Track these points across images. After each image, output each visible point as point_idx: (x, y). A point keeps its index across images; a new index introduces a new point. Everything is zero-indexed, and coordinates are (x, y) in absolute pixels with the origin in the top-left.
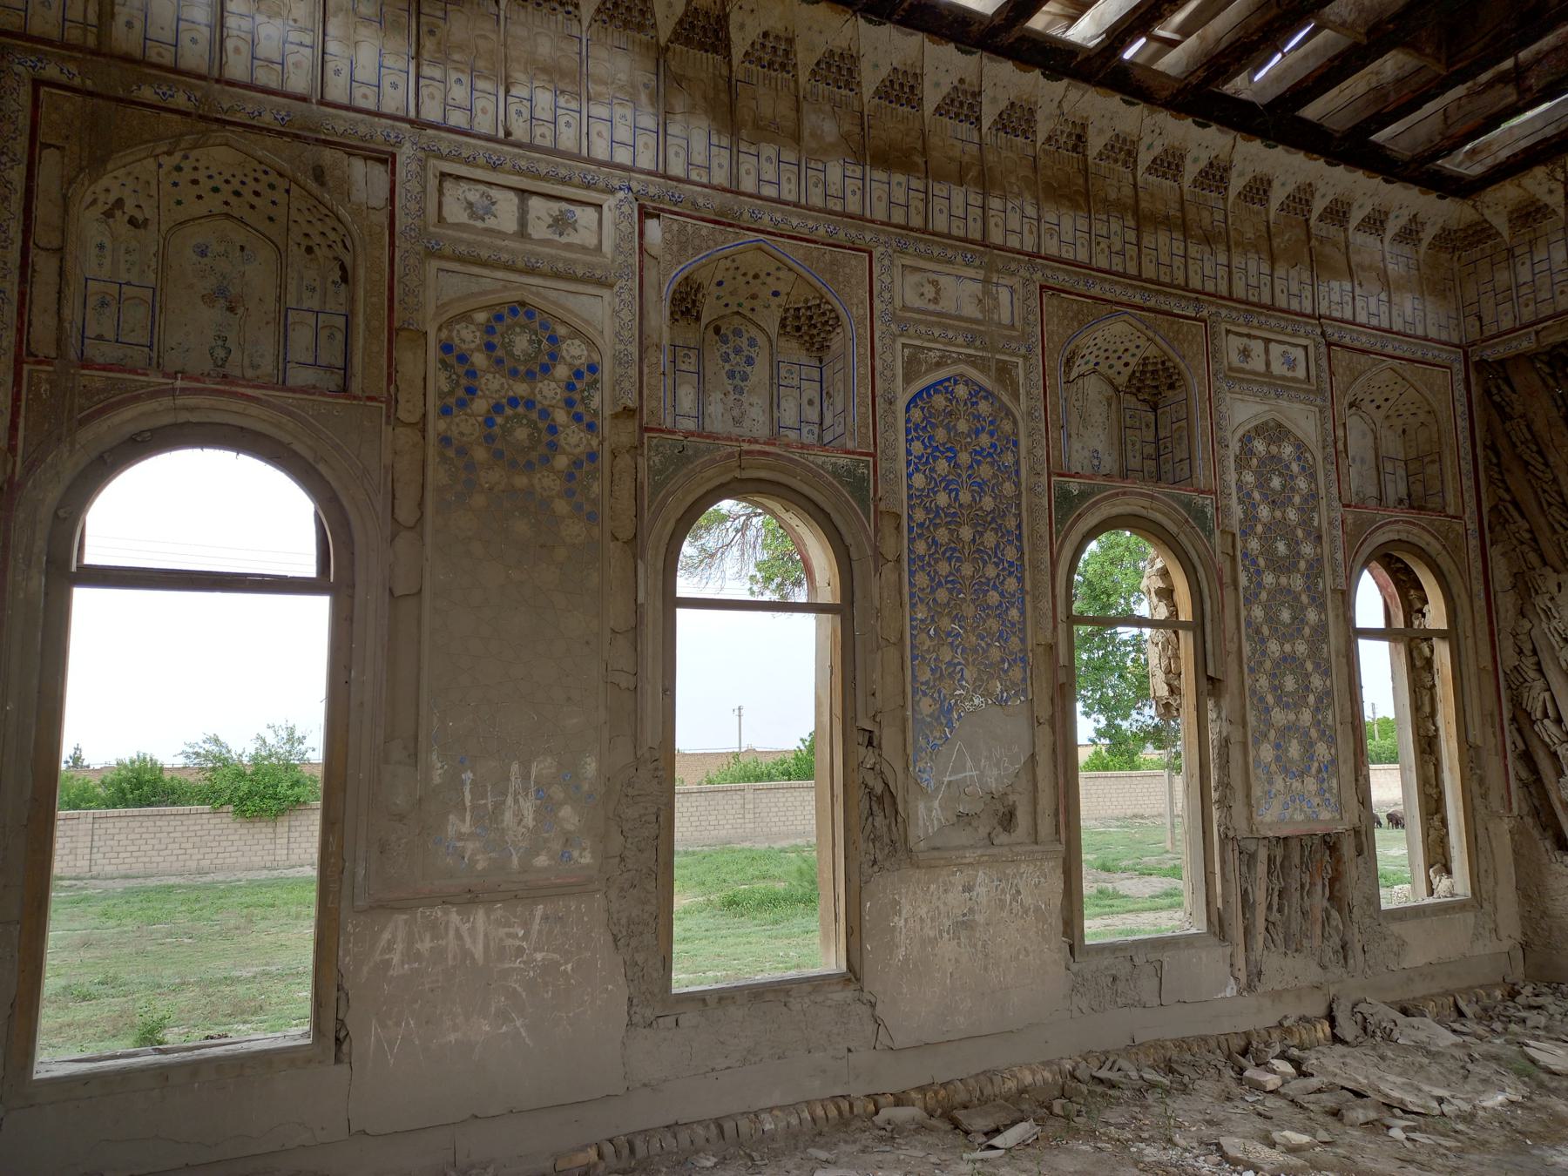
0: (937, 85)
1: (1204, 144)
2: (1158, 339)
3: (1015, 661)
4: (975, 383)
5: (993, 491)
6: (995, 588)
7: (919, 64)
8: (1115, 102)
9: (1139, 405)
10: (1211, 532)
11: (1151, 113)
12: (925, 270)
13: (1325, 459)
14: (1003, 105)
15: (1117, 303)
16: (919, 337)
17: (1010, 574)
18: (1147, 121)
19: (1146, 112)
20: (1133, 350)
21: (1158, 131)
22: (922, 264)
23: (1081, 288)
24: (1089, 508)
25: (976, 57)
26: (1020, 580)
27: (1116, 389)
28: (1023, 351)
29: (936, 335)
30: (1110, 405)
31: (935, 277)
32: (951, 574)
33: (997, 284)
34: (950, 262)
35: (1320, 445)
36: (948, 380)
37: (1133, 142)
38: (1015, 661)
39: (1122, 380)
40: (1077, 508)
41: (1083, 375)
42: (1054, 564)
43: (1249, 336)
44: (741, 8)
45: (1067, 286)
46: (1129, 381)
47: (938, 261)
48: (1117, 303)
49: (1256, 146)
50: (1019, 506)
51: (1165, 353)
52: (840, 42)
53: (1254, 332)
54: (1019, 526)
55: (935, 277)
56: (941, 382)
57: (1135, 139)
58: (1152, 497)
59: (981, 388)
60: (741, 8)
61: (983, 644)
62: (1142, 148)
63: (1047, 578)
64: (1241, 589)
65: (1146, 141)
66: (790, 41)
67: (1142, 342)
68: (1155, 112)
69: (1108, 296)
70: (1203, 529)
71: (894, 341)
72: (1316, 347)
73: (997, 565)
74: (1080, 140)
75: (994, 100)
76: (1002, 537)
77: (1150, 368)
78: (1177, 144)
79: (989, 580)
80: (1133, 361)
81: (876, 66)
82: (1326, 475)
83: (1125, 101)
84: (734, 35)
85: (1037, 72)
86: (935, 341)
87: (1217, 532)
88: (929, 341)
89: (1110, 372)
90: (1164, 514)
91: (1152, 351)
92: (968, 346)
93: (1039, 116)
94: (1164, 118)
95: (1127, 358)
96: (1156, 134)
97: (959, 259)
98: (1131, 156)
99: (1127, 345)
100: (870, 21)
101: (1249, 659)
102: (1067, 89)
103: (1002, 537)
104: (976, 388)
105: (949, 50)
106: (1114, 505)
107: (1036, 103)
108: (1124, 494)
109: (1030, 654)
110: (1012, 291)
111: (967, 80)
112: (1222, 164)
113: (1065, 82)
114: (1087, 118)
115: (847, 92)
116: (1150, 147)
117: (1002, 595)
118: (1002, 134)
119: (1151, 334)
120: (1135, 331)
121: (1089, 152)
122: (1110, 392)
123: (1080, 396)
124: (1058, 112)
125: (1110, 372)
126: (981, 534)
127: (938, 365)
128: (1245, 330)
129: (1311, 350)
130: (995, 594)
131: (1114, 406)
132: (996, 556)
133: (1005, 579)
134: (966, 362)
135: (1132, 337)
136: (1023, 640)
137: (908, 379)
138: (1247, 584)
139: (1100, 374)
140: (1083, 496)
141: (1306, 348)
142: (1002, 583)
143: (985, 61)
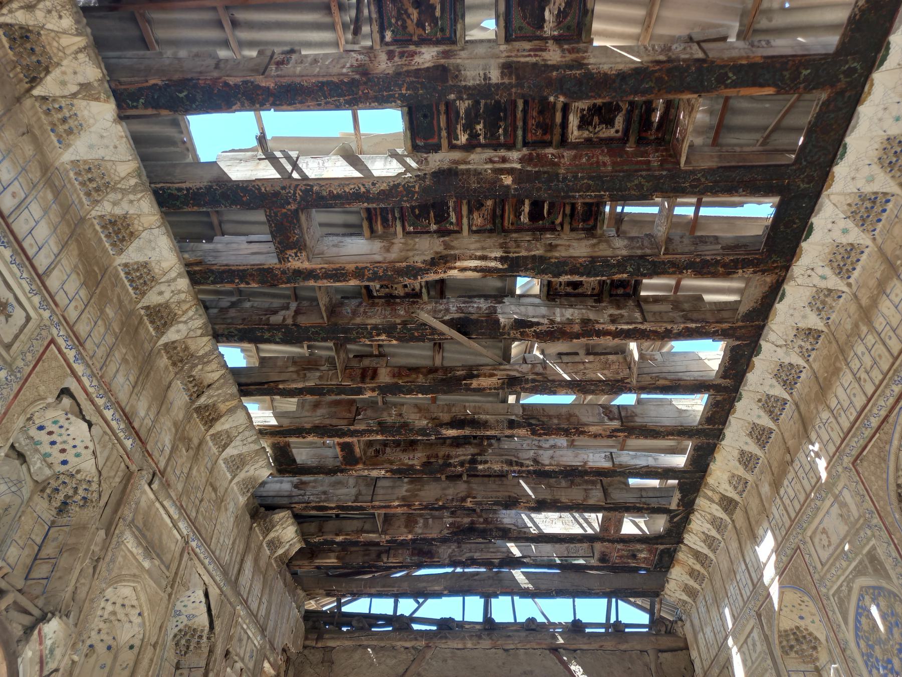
1: (830, 226)
8: (780, 308)
11: (793, 278)
16: (834, 582)
18: (799, 281)
19: (792, 283)
21: (809, 272)
23: (868, 433)
25: (743, 393)
45: (862, 443)
47: (816, 515)
49: (840, 170)
57: (815, 289)
62: (823, 284)
65: (816, 280)
69: (883, 413)
74: (811, 333)
75: (772, 386)
78: (827, 251)
81: (746, 443)
83: (781, 300)
93: (787, 361)
94: (798, 268)
96: (813, 274)
100: (723, 439)
105: (739, 405)
113: (762, 342)
124: (784, 348)
143: (746, 388)
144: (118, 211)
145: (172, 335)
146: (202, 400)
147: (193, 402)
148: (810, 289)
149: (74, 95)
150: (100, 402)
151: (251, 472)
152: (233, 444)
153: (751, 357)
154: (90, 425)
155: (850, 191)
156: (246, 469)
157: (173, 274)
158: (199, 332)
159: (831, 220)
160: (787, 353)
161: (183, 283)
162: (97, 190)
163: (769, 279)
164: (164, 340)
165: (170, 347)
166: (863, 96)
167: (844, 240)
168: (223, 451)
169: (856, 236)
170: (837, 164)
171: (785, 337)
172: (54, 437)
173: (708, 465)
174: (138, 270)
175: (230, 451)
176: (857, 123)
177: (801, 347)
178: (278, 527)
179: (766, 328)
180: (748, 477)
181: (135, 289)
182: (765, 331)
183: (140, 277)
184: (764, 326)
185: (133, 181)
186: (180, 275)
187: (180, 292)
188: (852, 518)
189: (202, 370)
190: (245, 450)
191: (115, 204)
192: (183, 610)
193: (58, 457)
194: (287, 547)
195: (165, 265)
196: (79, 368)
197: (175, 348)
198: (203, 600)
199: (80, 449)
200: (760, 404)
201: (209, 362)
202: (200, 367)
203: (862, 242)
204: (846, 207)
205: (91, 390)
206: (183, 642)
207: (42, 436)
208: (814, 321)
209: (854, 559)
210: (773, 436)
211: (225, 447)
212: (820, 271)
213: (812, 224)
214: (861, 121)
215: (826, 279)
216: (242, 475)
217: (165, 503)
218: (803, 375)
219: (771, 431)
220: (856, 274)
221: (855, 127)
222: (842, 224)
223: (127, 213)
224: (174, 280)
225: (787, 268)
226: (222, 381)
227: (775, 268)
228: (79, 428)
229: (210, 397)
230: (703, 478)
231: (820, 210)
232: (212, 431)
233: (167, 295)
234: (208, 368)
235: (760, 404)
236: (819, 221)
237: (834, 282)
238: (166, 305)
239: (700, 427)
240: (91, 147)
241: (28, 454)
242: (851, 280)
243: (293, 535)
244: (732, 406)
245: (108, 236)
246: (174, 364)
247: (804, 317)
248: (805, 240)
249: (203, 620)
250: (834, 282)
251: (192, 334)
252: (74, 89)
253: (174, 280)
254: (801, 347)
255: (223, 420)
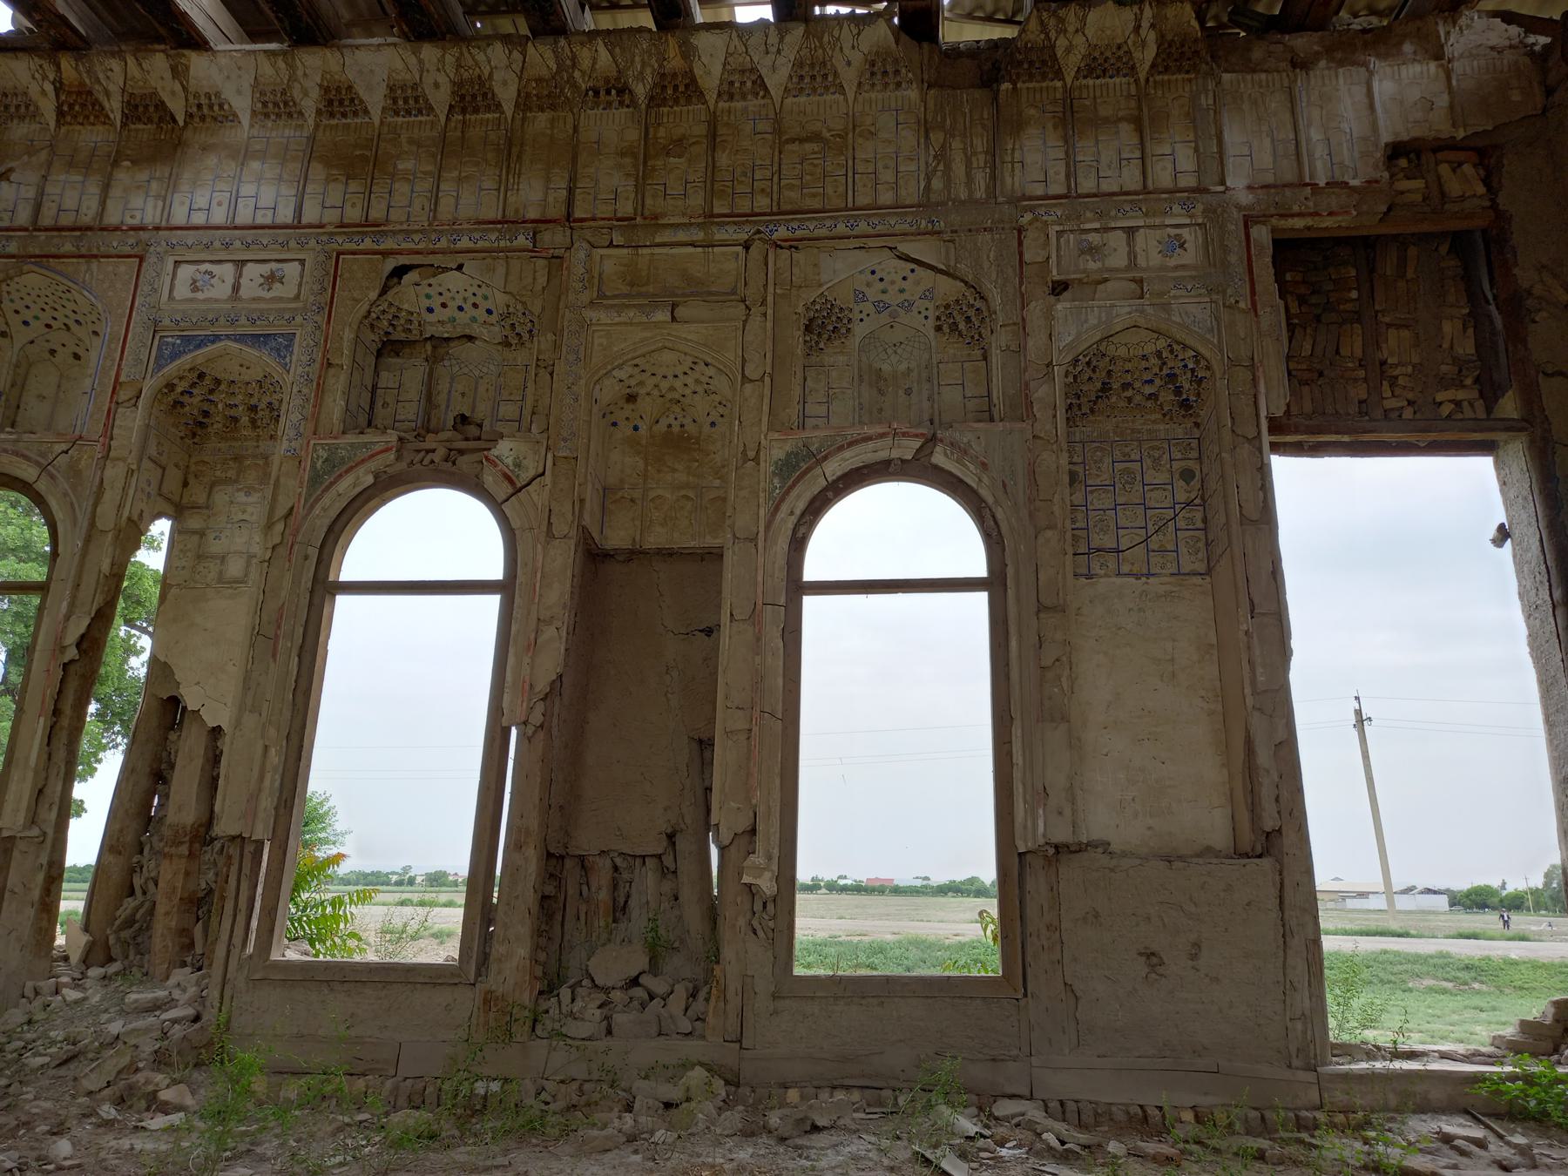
144: (315, 93)
145: (507, 94)
146: (641, 91)
147: (633, 103)
149: (185, 89)
150: (443, 243)
151: (857, 58)
152: (764, 72)
154: (460, 268)
156: (839, 63)
157: (413, 60)
158: (516, 55)
161: (429, 52)
162: (286, 104)
164: (508, 108)
165: (524, 103)
168: (766, 89)
172: (453, 305)
174: (395, 101)
175: (776, 81)
178: (1061, 43)
181: (420, 112)
183: (406, 101)
185: (281, 64)
186: (416, 53)
187: (442, 60)
189: (583, 73)
190: (790, 54)
191: (306, 94)
192: (905, 296)
193: (480, 314)
194: (1152, 37)
195: (399, 65)
196: (389, 244)
197: (528, 95)
198: (913, 266)
199: (479, 292)
201: (574, 58)
202: (577, 74)
205: (421, 246)
206: (962, 326)
207: (440, 314)
211: (760, 84)
216: (849, 77)
217: (658, 240)
223: (320, 86)
224: (421, 62)
226: (617, 50)
228: (452, 280)
229: (641, 77)
232: (711, 97)
233: (442, 79)
234: (586, 63)
238: (458, 85)
240: (239, 92)
241: (467, 332)
243: (1128, 14)
245: (344, 115)
246: (553, 107)
249: (948, 288)
251: (517, 67)
252: (178, 87)
253: (421, 62)
255: (698, 72)
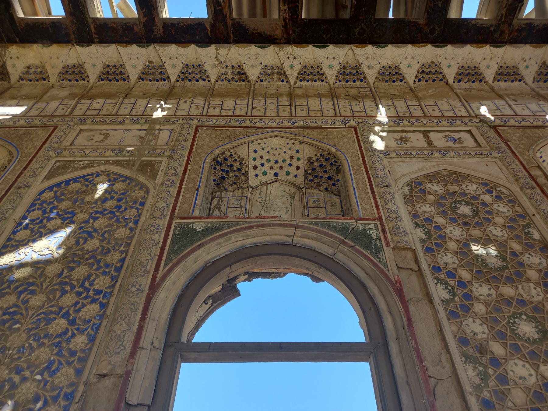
0: (134, 66)
2: (306, 139)
3: (55, 399)
4: (115, 174)
5: (103, 235)
6: (66, 316)
7: (120, 60)
8: (253, 49)
9: (322, 194)
10: (378, 251)
11: (281, 49)
12: (100, 130)
13: (521, 188)
14: (180, 67)
15: (266, 128)
17: (93, 301)
18: (281, 53)
19: (277, 50)
20: (296, 155)
21: (292, 57)
22: (97, 127)
24: (213, 240)
26: (103, 306)
27: (299, 188)
28: (167, 153)
29: (87, 152)
30: (292, 197)
31: (107, 132)
32: (15, 305)
33: (160, 130)
34: (120, 123)
35: (512, 179)
36: (92, 175)
37: (279, 68)
38: (55, 399)
39: (300, 180)
40: (198, 240)
41: (266, 184)
42: (154, 287)
43: (404, 131)
44: (11, 58)
45: (222, 124)
46: (306, 178)
47: (110, 124)
48: (266, 128)
49: (370, 49)
50: (128, 245)
51: (318, 148)
52: (72, 61)
53: (407, 129)
54: (123, 260)
55: (107, 132)
56: (83, 177)
57: (280, 65)
58: (296, 226)
59: (121, 176)
60: (11, 58)
61: (17, 379)
62: (287, 68)
63: (141, 301)
64: (437, 301)
66: (43, 67)
67: (297, 147)
68: (284, 47)
70: (368, 247)
71: (48, 160)
72: (479, 128)
73: (79, 294)
74: (242, 75)
75: (174, 66)
76: (97, 269)
77: (316, 164)
78: (312, 62)
79: (61, 309)
80: (300, 164)
82: (530, 198)
83: (259, 47)
84: (10, 70)
85: (193, 46)
86: (87, 156)
87: (388, 252)
88: (81, 156)
89: (289, 177)
90: (312, 239)
91: (309, 152)
92: (118, 156)
94: (291, 49)
95: (295, 163)
96: (292, 60)
97: (127, 121)
98: (282, 75)
99: (290, 153)
101: (478, 388)
102: (216, 49)
103: (97, 269)
104: (116, 177)
105: (134, 48)
106: (248, 237)
107: (201, 62)
108: (261, 226)
109: (81, 388)
110: (172, 131)
111: (154, 61)
112: (354, 66)
113: (213, 46)
114: (240, 62)
115: (82, 82)
116: (292, 67)
117: (72, 323)
118: (188, 83)
119: (301, 138)
120: (288, 141)
121: (250, 79)
122: (293, 190)
123: (263, 195)
125: (289, 177)
126: (72, 269)
127: (84, 168)
128: (399, 129)
129: (475, 132)
130: (63, 321)
131: (297, 198)
132: (82, 285)
133: (84, 305)
134: (113, 164)
135: (289, 146)
136: (79, 372)
137: (49, 177)
138: (447, 296)
139: (282, 181)
140: (207, 231)
141: (469, 132)
142: (79, 310)
143: (158, 48)
148: (278, 61)
153: (193, 43)
155: (359, 59)
159: (335, 56)
160: (214, 66)
163: (278, 32)
166: (417, 44)
167: (325, 69)
169: (331, 74)
170: (373, 46)
171: (227, 60)
173: (34, 42)
176: (401, 47)
177: (226, 73)
179: (229, 45)
180: (53, 79)
182: (226, 45)
184: (230, 43)
188: (153, 143)
200: (147, 64)
203: (329, 78)
204: (345, 61)
208: (253, 74)
209: (124, 156)
210: (121, 82)
212: (296, 63)
213: (328, 46)
214: (402, 49)
215: (291, 68)
218: (201, 82)
219: (126, 79)
220: (304, 83)
221: (398, 47)
222: (335, 63)
225: (288, 42)
227: (288, 34)
230: (12, 42)
231: (339, 47)
235: (147, 64)
236: (331, 49)
237: (292, 75)
239: (90, 21)
242: (299, 83)
244: (129, 42)
247: (253, 66)
248: (314, 46)
250: (292, 75)
254: (226, 73)
